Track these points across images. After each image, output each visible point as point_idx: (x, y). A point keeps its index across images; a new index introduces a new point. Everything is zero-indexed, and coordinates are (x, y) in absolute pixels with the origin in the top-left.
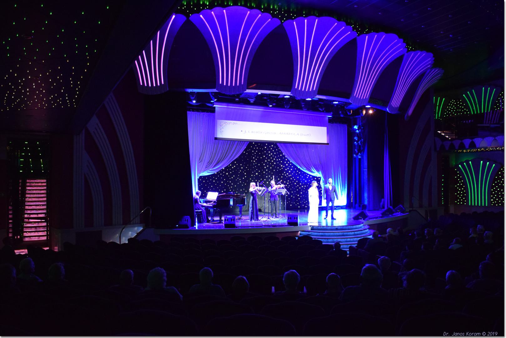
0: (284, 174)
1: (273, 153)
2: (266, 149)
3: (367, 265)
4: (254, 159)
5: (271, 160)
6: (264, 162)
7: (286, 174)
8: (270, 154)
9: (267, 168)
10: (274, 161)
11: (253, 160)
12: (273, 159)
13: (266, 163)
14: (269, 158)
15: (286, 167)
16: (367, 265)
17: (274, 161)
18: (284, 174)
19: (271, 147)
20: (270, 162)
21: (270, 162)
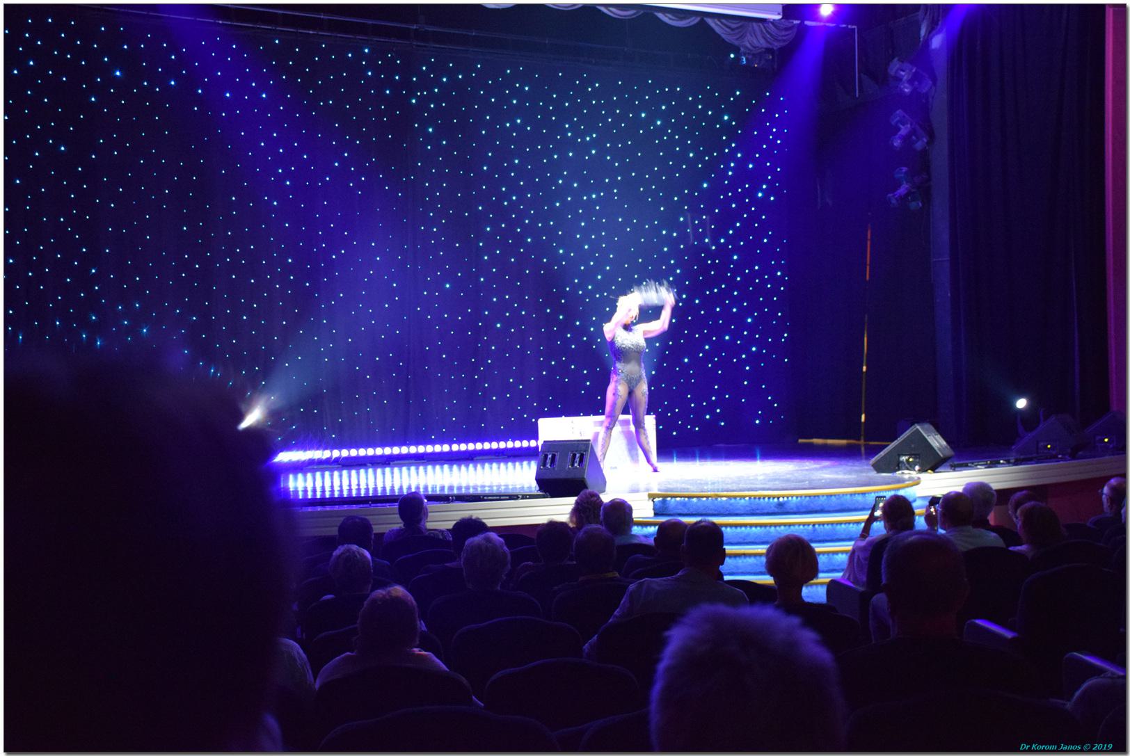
0: (575, 288)
1: (521, 192)
2: (487, 177)
3: (399, 590)
4: (433, 222)
5: (512, 224)
6: (481, 235)
7: (582, 285)
8: (506, 196)
9: (494, 260)
10: (528, 231)
11: (431, 223)
12: (519, 222)
13: (489, 238)
14: (502, 214)
15: (584, 257)
16: (399, 590)
17: (528, 231)
18: (575, 288)
19: (512, 167)
20: (510, 231)
21: (510, 231)
